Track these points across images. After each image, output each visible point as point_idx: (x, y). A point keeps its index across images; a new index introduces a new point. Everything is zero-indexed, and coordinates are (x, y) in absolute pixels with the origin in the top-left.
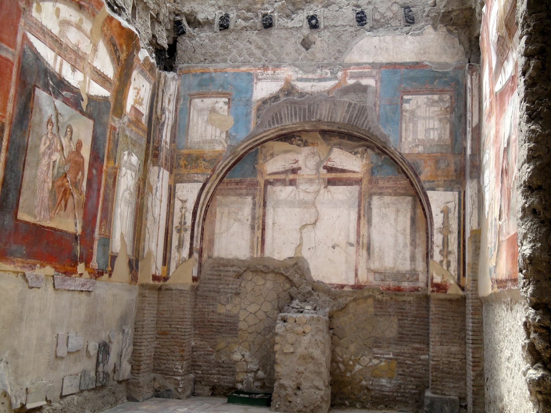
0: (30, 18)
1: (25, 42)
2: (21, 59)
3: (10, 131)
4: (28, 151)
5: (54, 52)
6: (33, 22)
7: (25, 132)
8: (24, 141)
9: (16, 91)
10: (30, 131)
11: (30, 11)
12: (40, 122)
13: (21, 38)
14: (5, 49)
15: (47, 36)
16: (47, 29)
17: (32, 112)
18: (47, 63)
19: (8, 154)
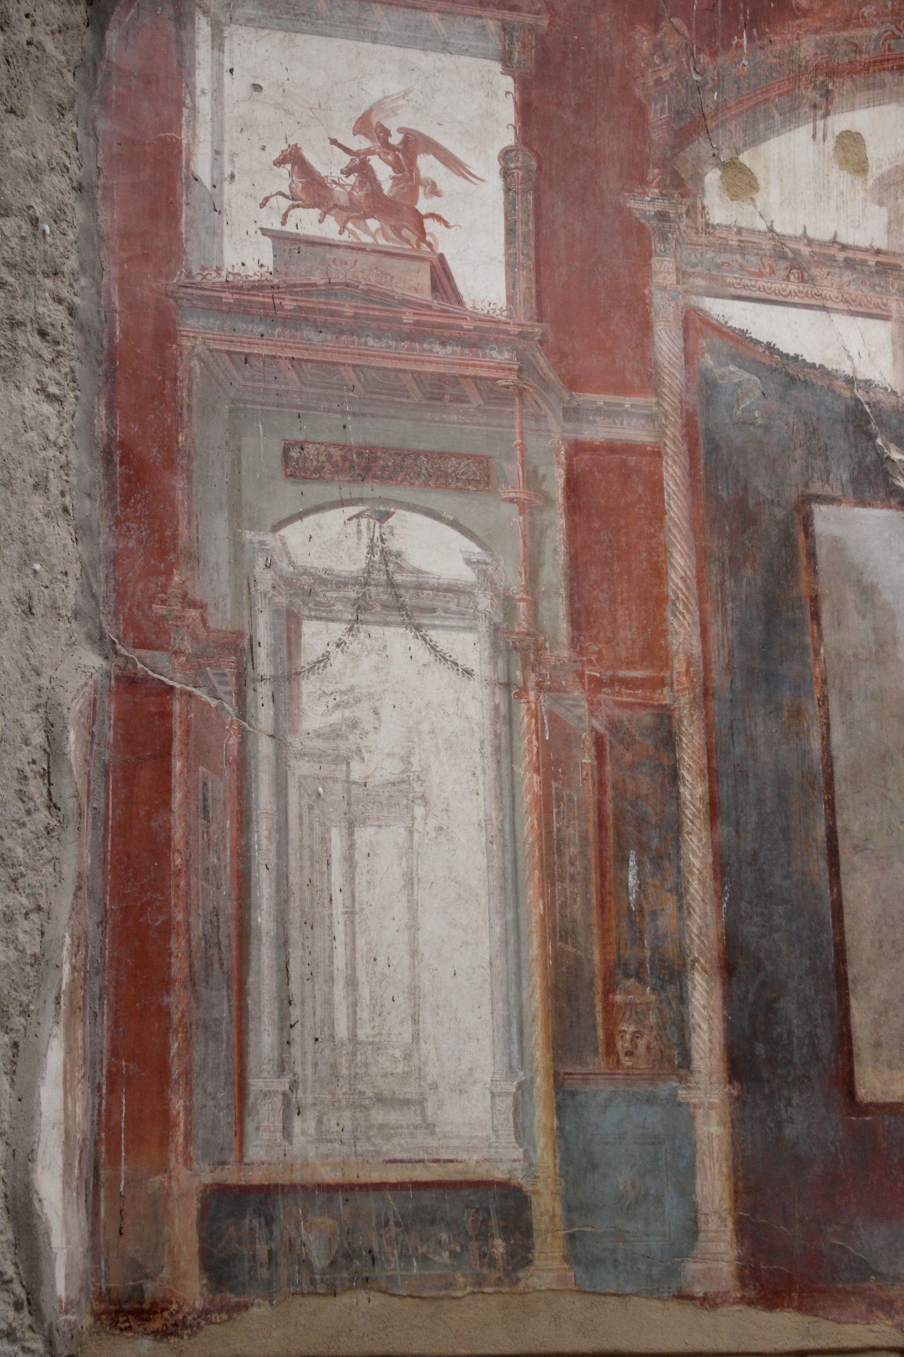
0: (703, 239)
1: (703, 343)
2: (700, 422)
3: (708, 728)
4: (840, 787)
5: (886, 318)
6: (724, 247)
7: (797, 713)
8: (805, 754)
9: (702, 556)
10: (824, 701)
11: (695, 210)
12: (881, 645)
13: (677, 332)
14: (598, 411)
15: (814, 271)
16: (810, 242)
17: (816, 616)
18: (850, 381)
19: (725, 831)
